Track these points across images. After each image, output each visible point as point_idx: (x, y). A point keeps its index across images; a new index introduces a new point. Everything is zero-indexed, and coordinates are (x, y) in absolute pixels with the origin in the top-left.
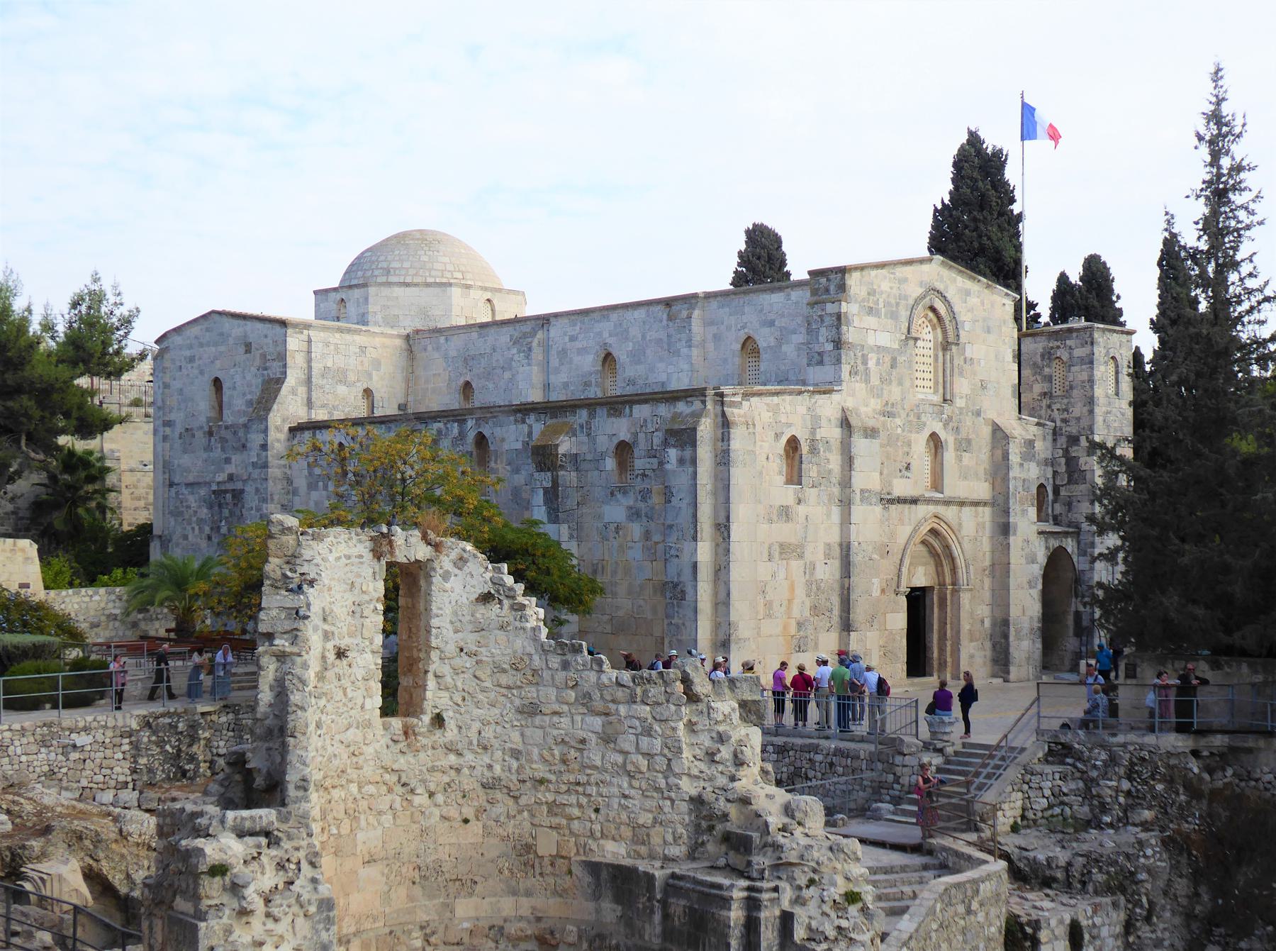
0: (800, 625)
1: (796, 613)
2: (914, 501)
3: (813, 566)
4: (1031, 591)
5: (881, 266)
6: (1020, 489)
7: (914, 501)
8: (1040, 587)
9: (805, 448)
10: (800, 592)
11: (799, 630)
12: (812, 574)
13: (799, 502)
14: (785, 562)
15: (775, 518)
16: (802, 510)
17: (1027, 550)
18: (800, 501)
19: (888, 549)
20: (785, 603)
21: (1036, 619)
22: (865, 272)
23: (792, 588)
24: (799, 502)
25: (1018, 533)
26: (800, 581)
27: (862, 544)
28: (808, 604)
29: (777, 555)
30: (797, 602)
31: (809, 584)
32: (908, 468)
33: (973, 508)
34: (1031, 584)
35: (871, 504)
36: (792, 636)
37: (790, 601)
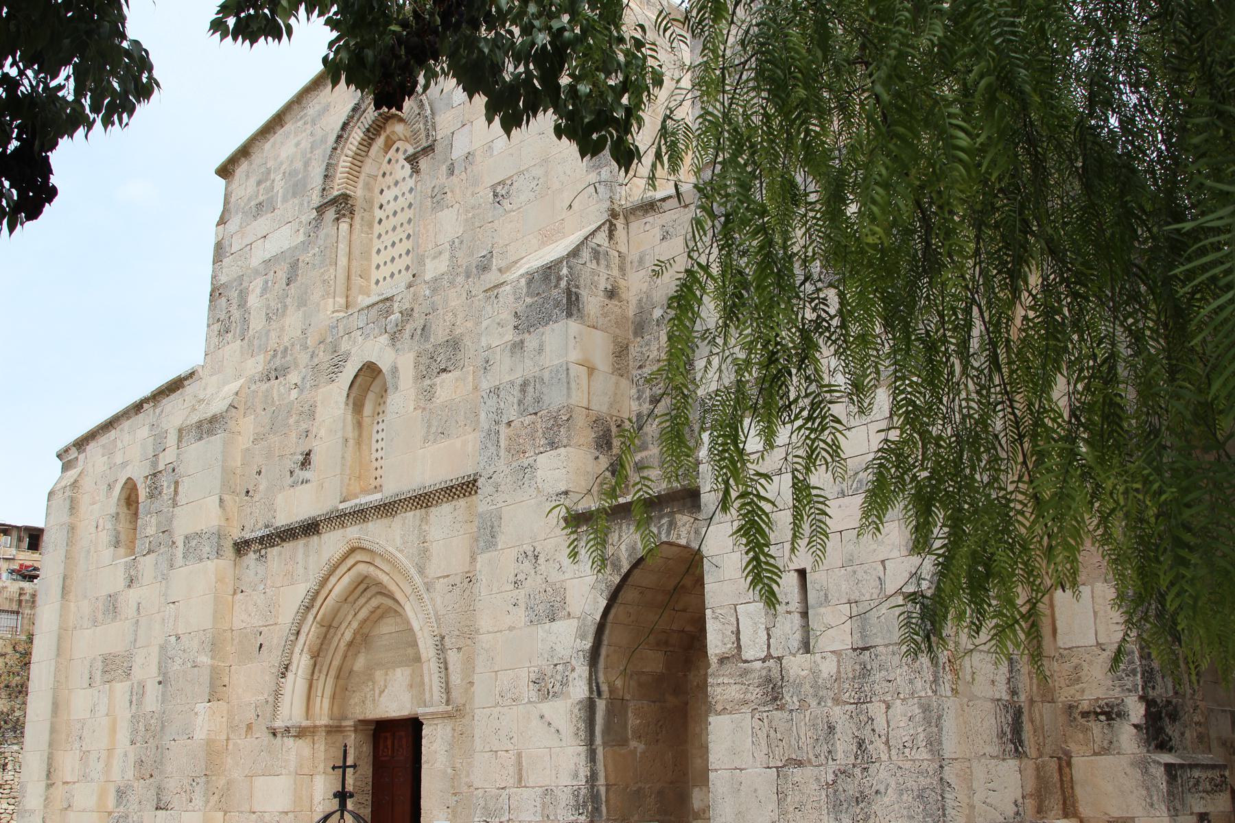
0: (121, 794)
1: (116, 775)
2: (311, 528)
3: (139, 693)
4: (547, 708)
5: (277, 121)
6: (512, 413)
7: (311, 528)
8: (579, 689)
9: (143, 493)
10: (123, 737)
11: (119, 804)
12: (140, 703)
13: (131, 582)
14: (107, 686)
15: (100, 617)
16: (133, 595)
17: (533, 583)
18: (132, 581)
19: (260, 640)
20: (104, 754)
21: (565, 797)
22: (257, 157)
23: (113, 730)
24: (131, 582)
25: (501, 541)
26: (124, 714)
27: (183, 638)
28: (132, 759)
29: (98, 675)
30: (119, 752)
31: (135, 718)
32: (306, 462)
33: (462, 503)
34: (545, 688)
35: (201, 560)
36: (110, 813)
37: (110, 751)
